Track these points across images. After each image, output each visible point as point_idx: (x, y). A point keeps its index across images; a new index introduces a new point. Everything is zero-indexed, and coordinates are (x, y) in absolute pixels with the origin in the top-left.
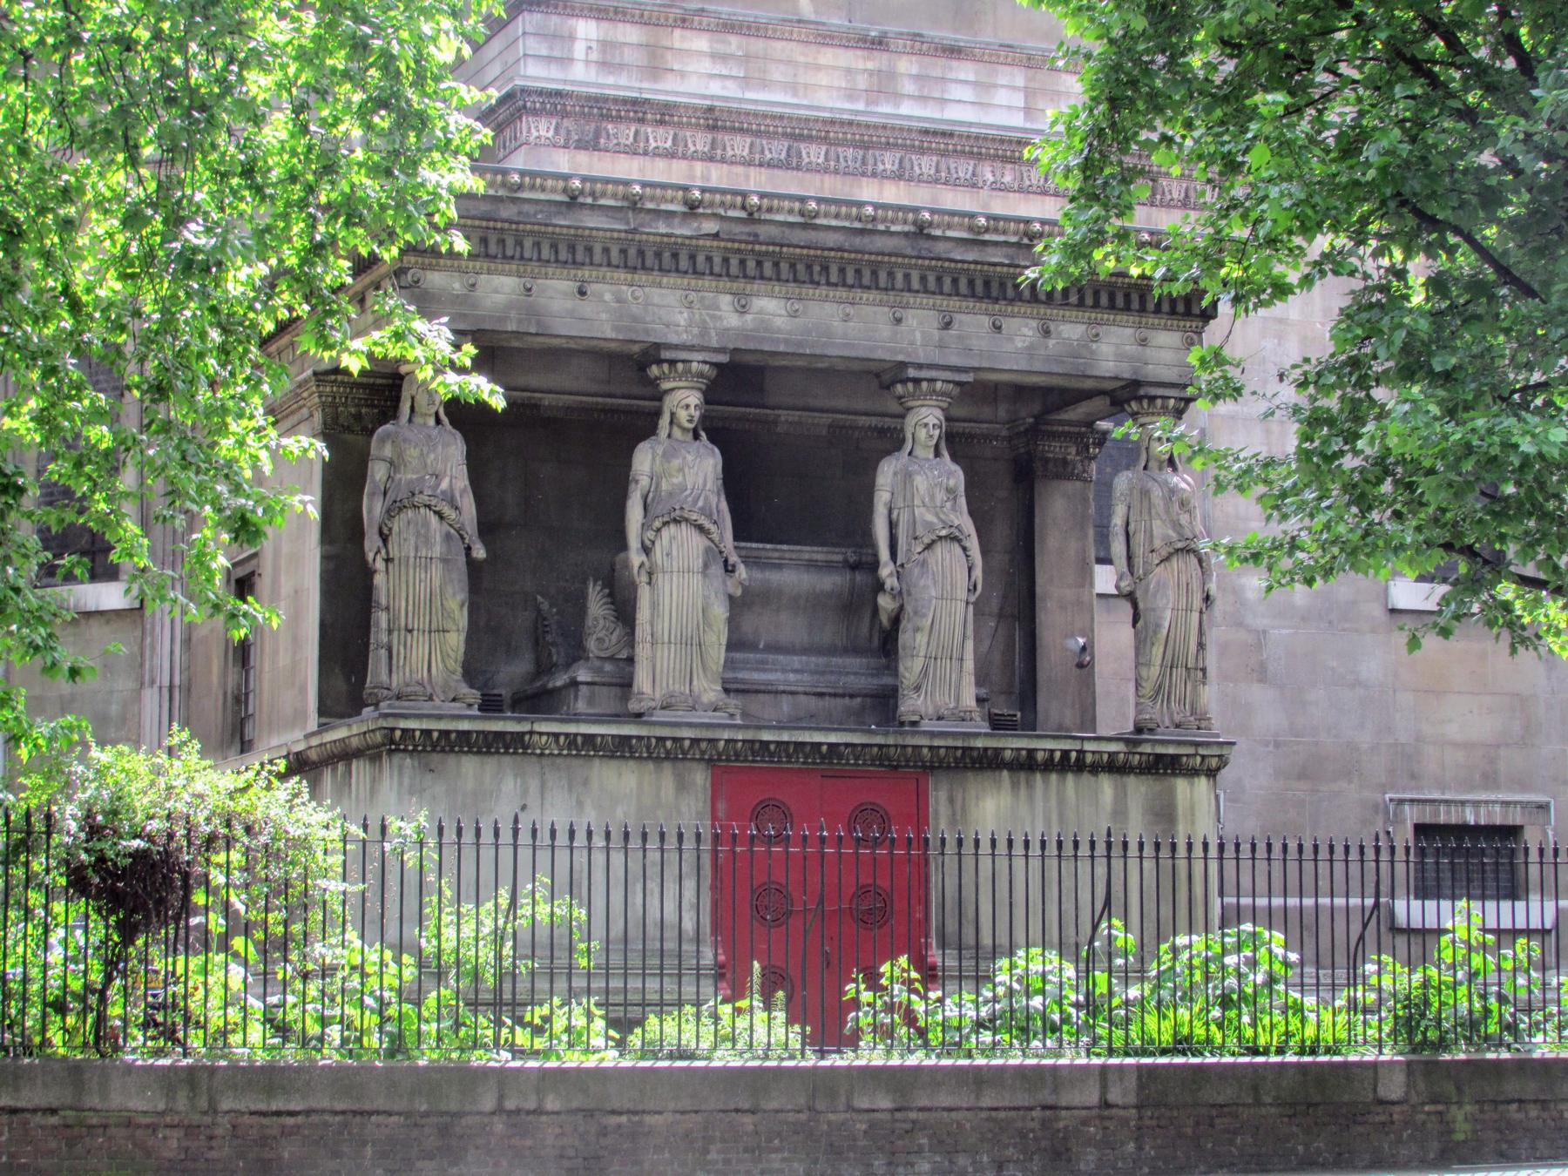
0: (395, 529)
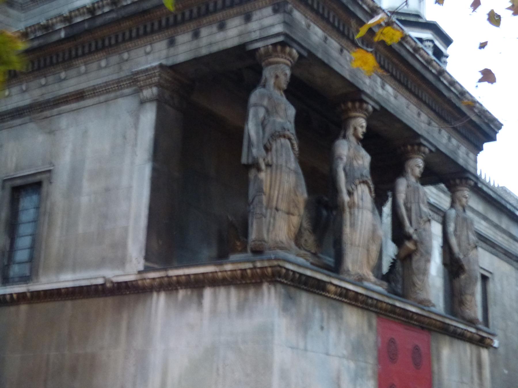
0: (274, 147)
